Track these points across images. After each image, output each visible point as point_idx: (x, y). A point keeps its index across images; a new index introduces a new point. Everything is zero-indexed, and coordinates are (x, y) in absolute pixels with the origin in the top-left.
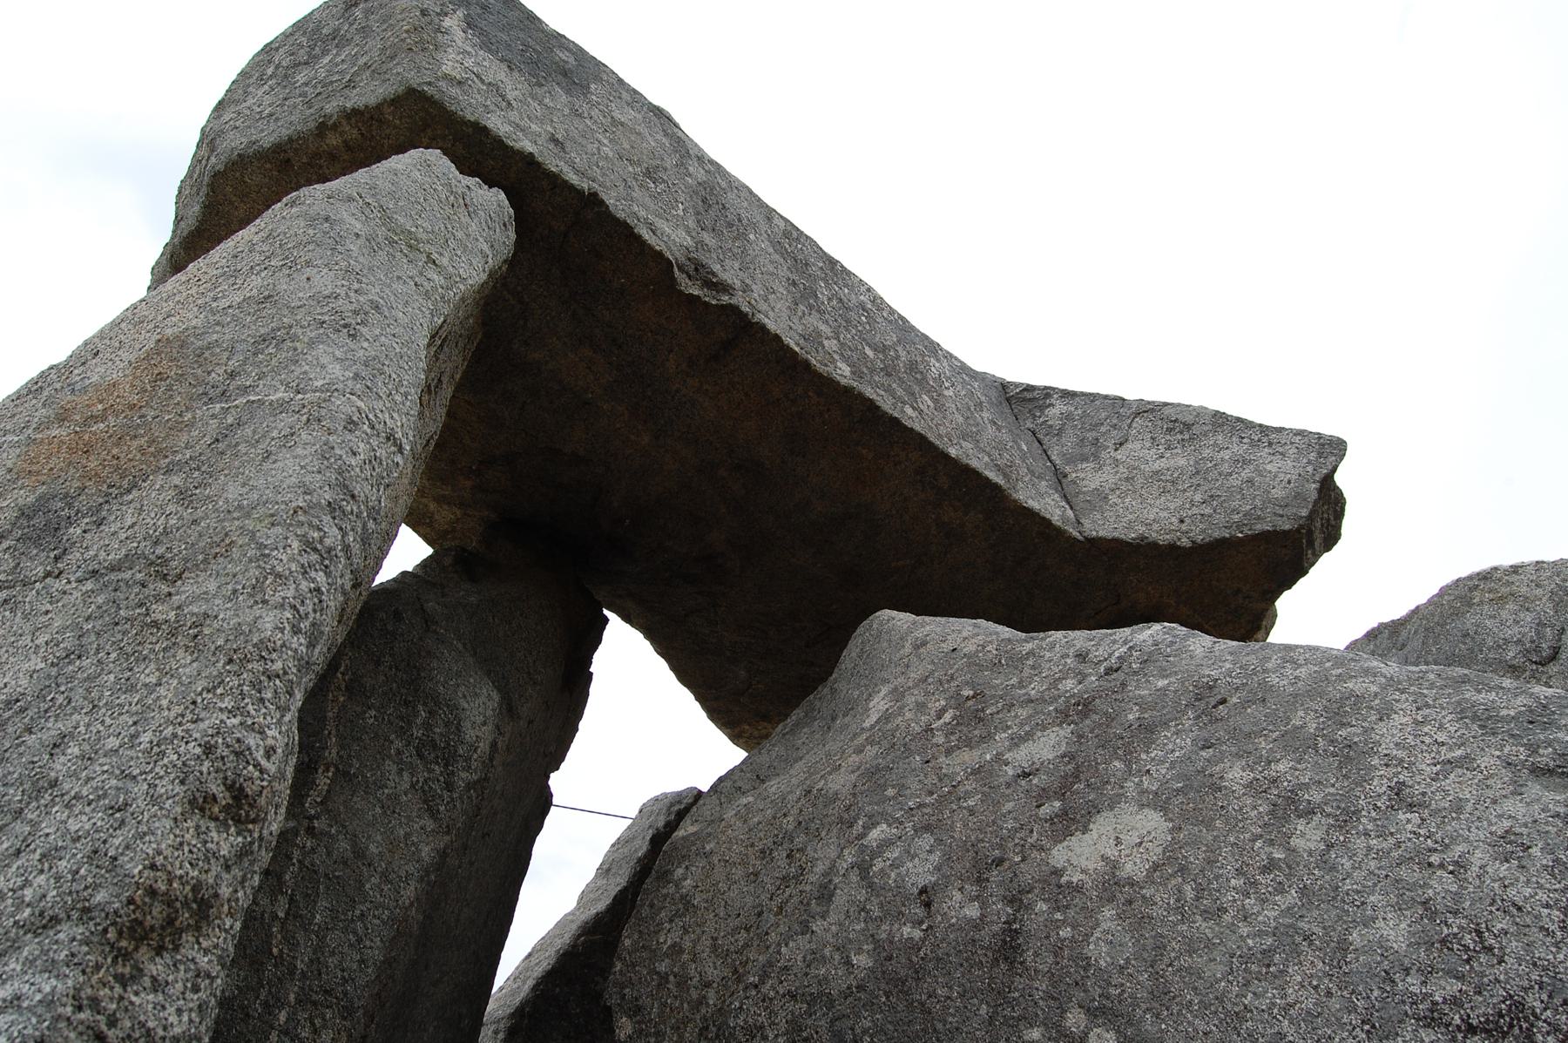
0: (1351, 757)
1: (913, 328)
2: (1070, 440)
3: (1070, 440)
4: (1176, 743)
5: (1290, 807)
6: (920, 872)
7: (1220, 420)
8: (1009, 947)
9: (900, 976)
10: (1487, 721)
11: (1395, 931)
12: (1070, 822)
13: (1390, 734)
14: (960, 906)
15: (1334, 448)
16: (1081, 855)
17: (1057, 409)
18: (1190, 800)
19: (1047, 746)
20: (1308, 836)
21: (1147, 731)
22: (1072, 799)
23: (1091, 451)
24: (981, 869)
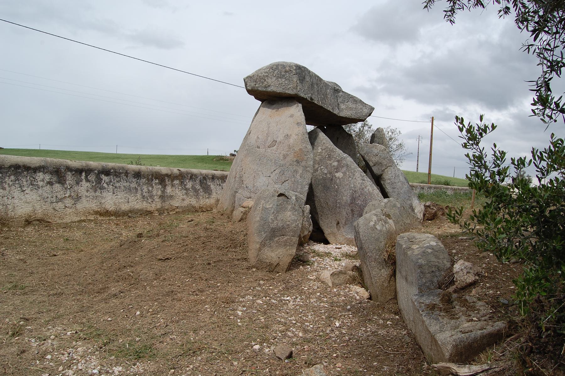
0: (354, 175)
1: (326, 85)
2: (341, 99)
3: (341, 99)
4: (344, 169)
5: (350, 177)
6: (326, 172)
7: (361, 101)
8: (332, 179)
9: (324, 179)
10: (361, 175)
11: (352, 186)
12: (337, 172)
13: (356, 174)
14: (328, 175)
15: (373, 109)
16: (337, 175)
17: (341, 94)
18: (344, 173)
19: (336, 164)
20: (350, 179)
21: (343, 167)
22: (337, 169)
23: (343, 102)
24: (330, 173)
